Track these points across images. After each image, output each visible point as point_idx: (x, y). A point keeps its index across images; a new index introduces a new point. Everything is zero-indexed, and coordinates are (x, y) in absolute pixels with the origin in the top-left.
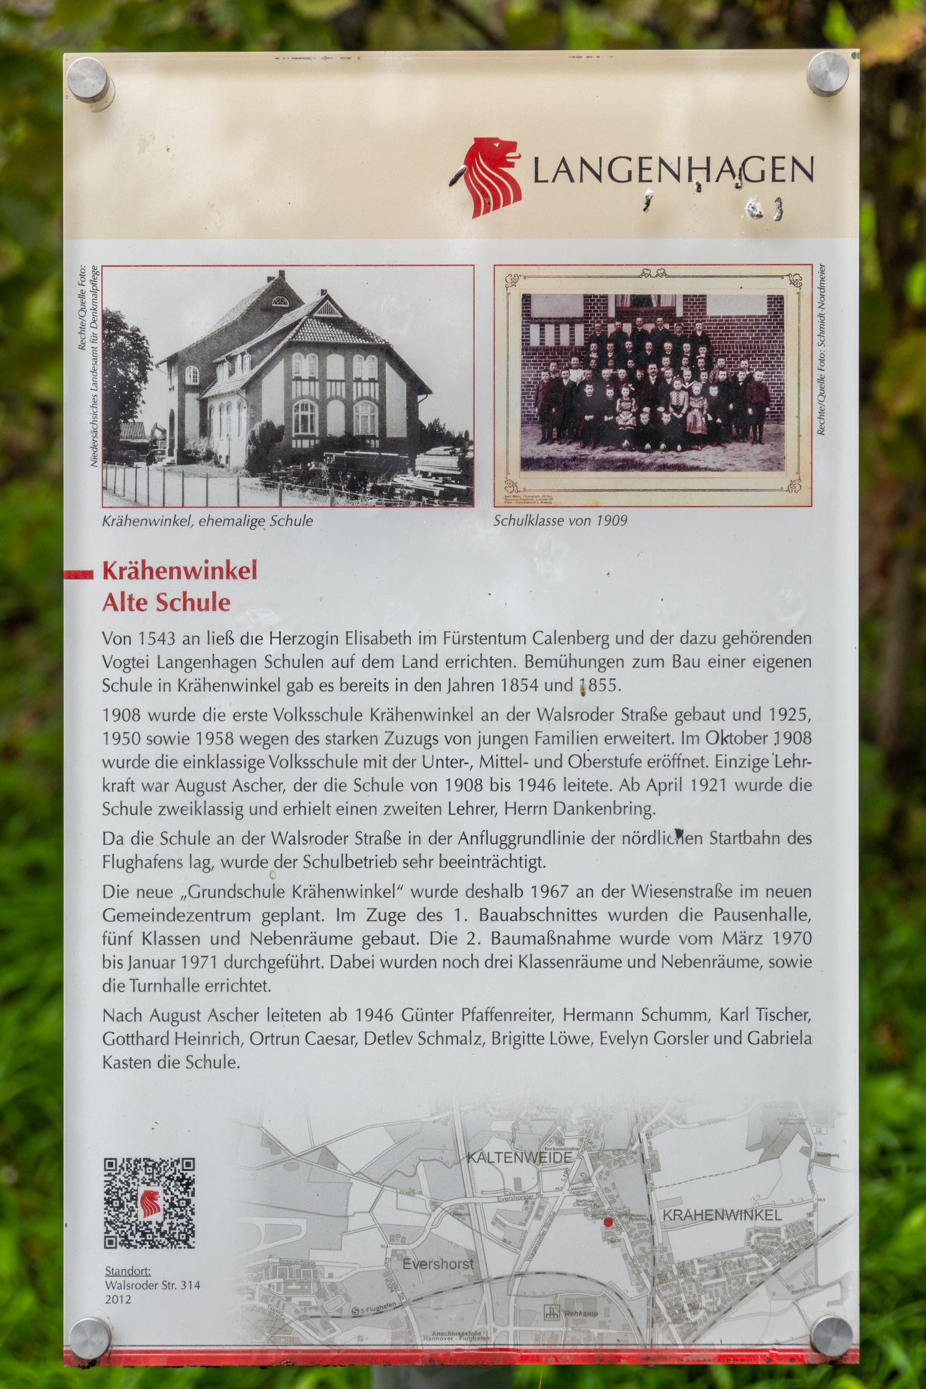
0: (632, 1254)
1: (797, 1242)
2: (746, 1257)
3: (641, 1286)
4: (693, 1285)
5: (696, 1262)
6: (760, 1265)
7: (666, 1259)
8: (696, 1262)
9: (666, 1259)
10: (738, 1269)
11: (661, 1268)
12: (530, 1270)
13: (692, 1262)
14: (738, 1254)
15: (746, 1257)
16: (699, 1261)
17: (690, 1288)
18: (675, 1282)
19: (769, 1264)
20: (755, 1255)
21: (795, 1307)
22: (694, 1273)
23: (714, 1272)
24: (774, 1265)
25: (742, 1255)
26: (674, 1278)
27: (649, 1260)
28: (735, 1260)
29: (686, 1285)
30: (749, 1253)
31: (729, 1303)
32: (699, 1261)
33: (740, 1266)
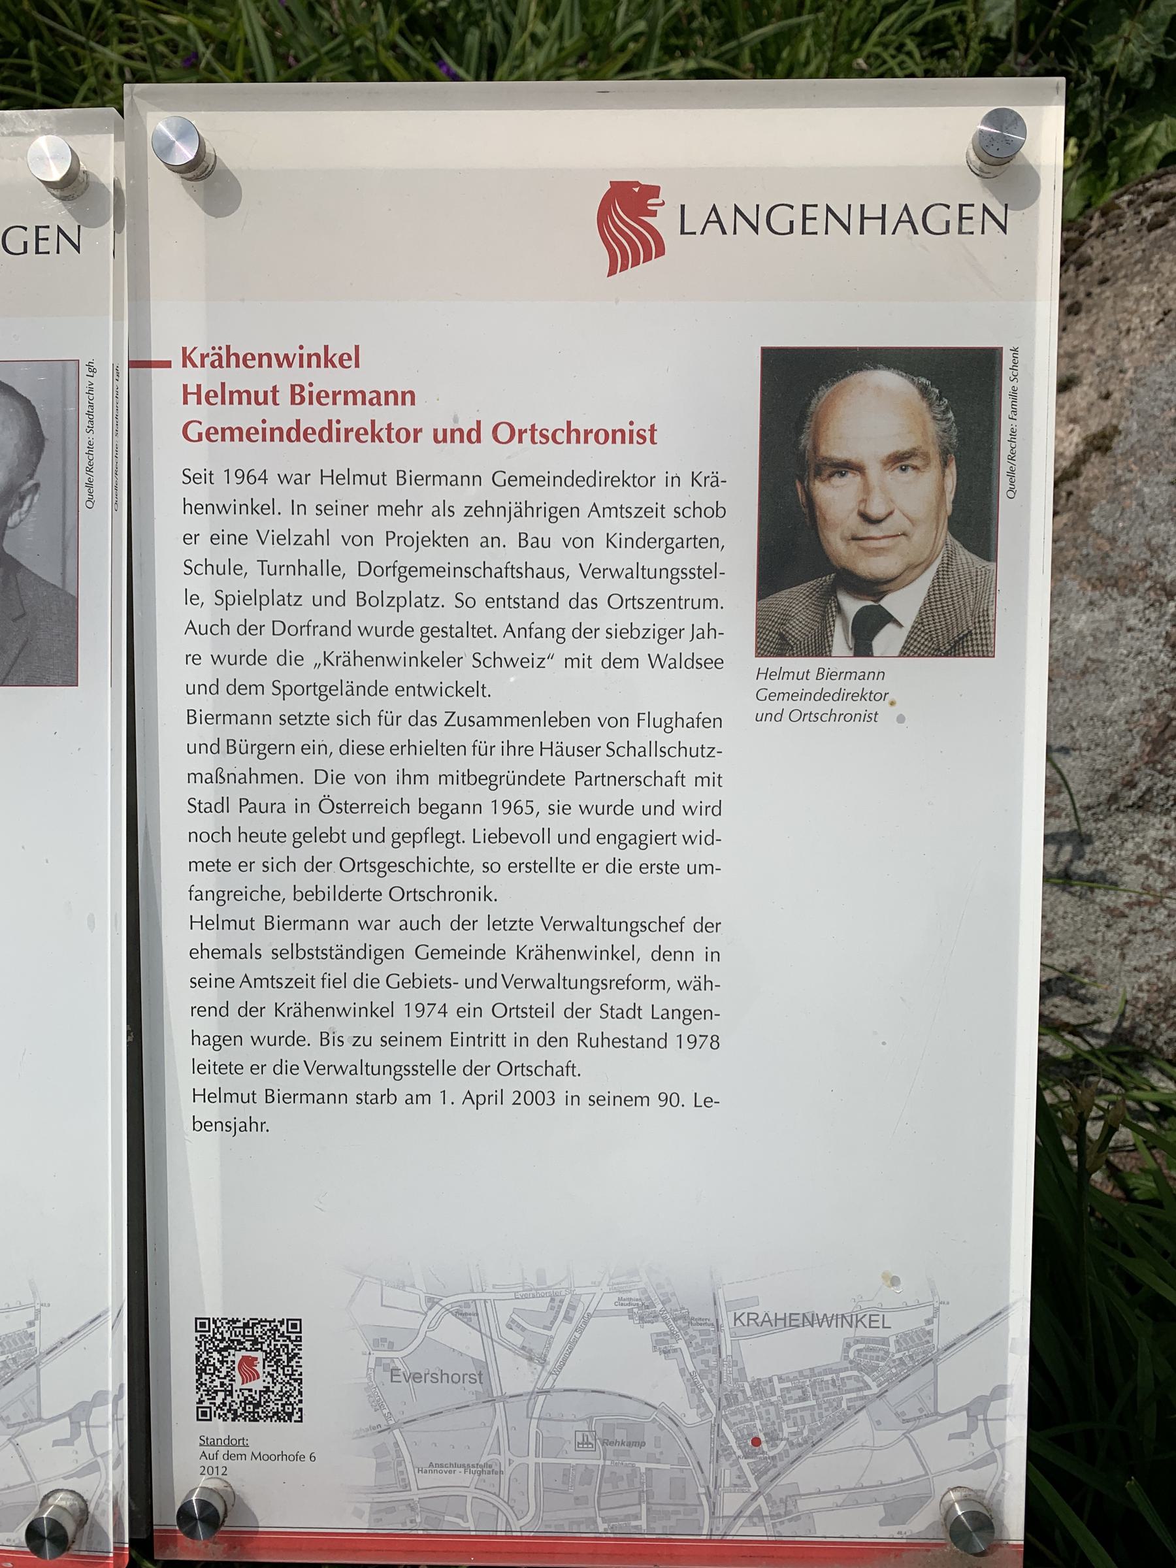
0: (691, 1369)
1: (911, 1357)
2: (842, 1375)
3: (702, 1410)
4: (772, 1408)
5: (775, 1379)
6: (861, 1385)
7: (736, 1375)
8: (775, 1379)
9: (736, 1375)
10: (832, 1389)
11: (729, 1386)
12: (558, 1386)
13: (771, 1380)
14: (831, 1371)
15: (842, 1375)
16: (781, 1379)
17: (768, 1412)
18: (748, 1405)
19: (873, 1385)
20: (856, 1373)
21: (906, 1440)
22: (773, 1394)
23: (799, 1393)
24: (879, 1386)
25: (838, 1372)
26: (747, 1400)
27: (713, 1376)
28: (828, 1378)
29: (762, 1409)
30: (846, 1369)
31: (819, 1434)
32: (781, 1379)
33: (834, 1385)
